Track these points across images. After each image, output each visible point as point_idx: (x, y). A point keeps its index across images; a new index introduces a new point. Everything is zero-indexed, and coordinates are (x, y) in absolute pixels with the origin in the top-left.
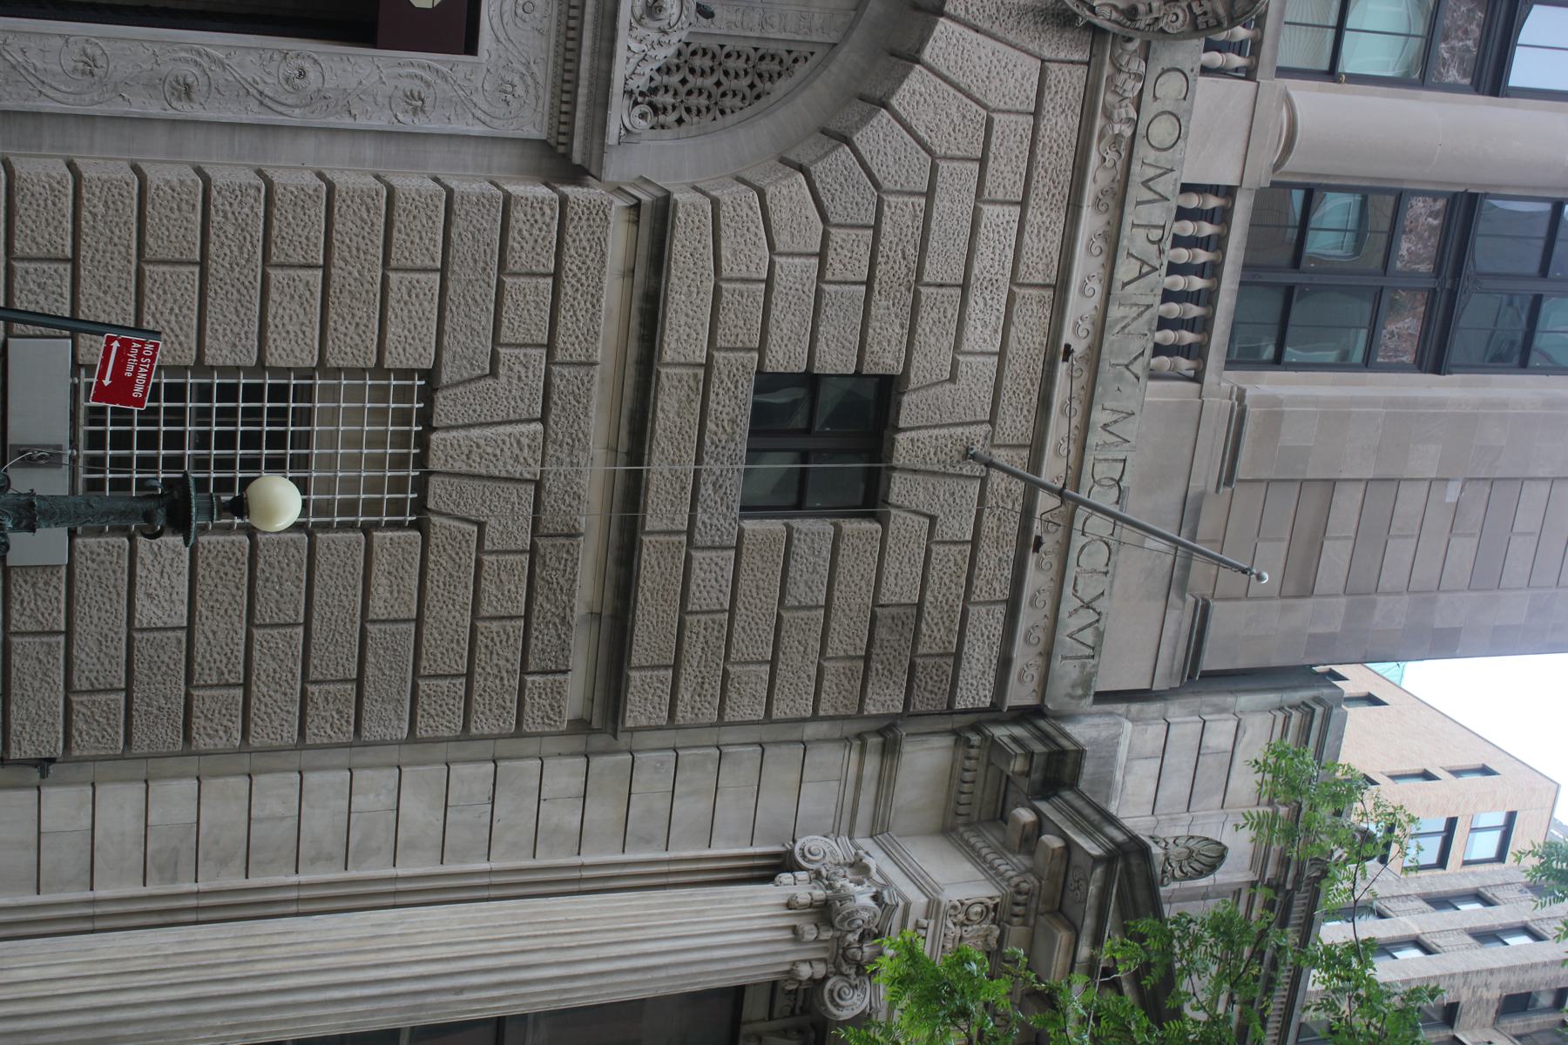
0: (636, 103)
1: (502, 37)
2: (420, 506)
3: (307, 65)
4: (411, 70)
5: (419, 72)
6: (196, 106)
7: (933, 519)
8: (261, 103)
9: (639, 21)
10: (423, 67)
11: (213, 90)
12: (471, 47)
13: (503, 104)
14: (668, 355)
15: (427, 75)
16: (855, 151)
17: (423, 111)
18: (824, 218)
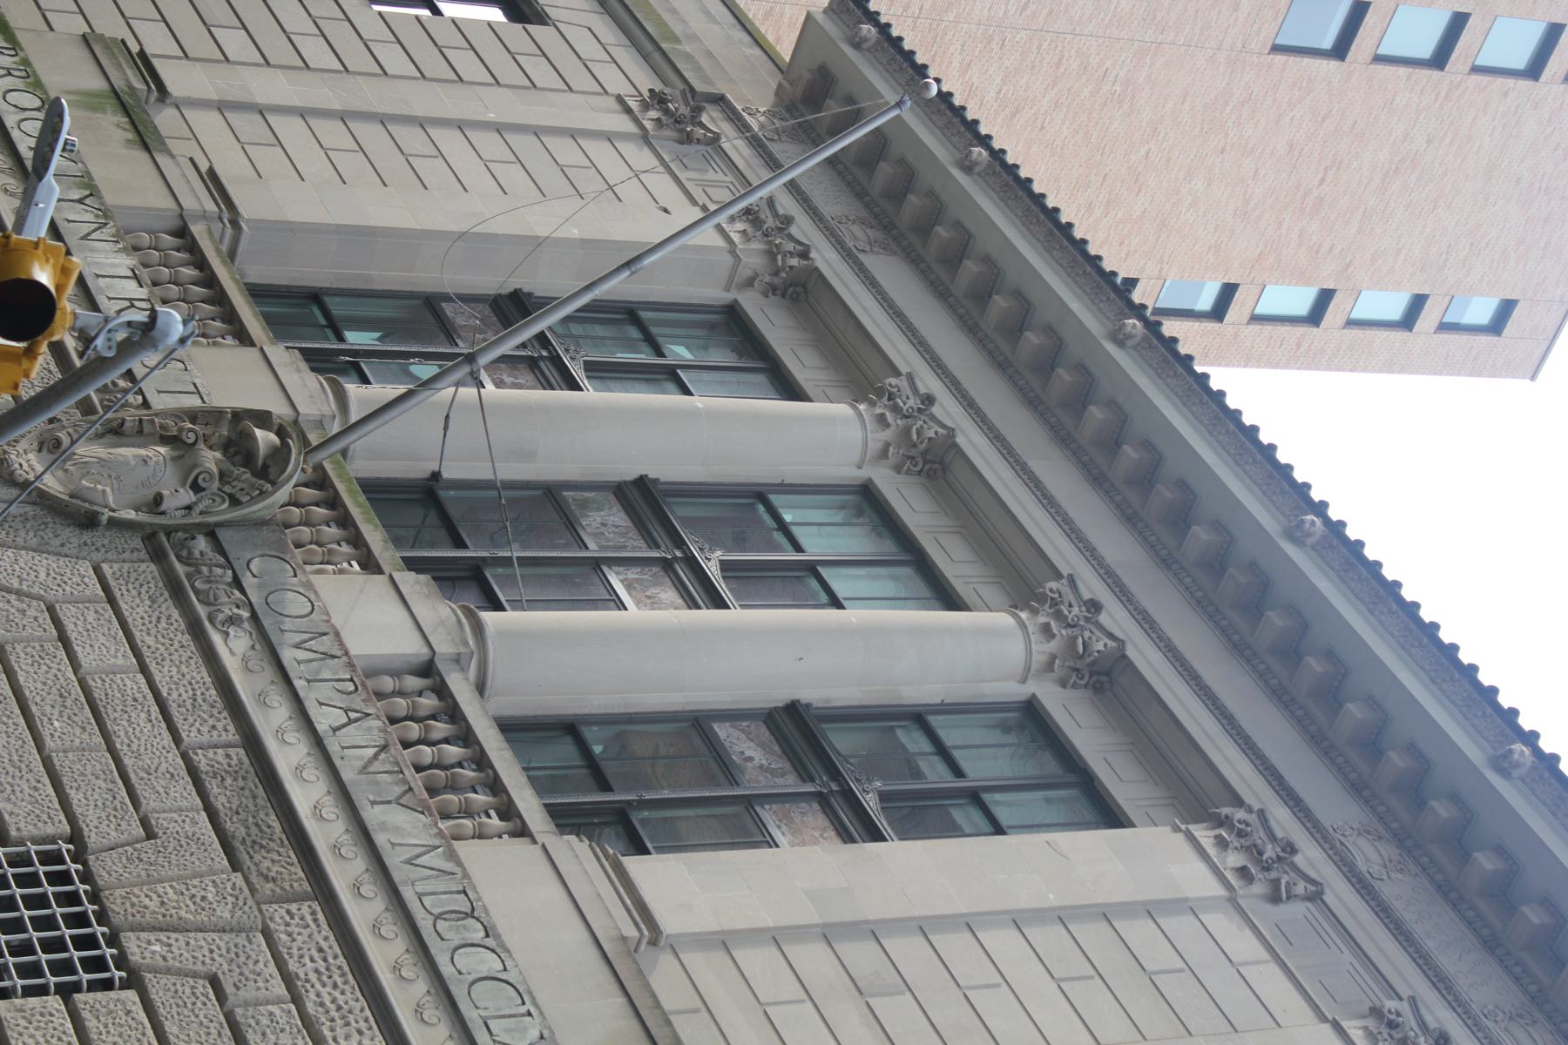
7: (215, 982)
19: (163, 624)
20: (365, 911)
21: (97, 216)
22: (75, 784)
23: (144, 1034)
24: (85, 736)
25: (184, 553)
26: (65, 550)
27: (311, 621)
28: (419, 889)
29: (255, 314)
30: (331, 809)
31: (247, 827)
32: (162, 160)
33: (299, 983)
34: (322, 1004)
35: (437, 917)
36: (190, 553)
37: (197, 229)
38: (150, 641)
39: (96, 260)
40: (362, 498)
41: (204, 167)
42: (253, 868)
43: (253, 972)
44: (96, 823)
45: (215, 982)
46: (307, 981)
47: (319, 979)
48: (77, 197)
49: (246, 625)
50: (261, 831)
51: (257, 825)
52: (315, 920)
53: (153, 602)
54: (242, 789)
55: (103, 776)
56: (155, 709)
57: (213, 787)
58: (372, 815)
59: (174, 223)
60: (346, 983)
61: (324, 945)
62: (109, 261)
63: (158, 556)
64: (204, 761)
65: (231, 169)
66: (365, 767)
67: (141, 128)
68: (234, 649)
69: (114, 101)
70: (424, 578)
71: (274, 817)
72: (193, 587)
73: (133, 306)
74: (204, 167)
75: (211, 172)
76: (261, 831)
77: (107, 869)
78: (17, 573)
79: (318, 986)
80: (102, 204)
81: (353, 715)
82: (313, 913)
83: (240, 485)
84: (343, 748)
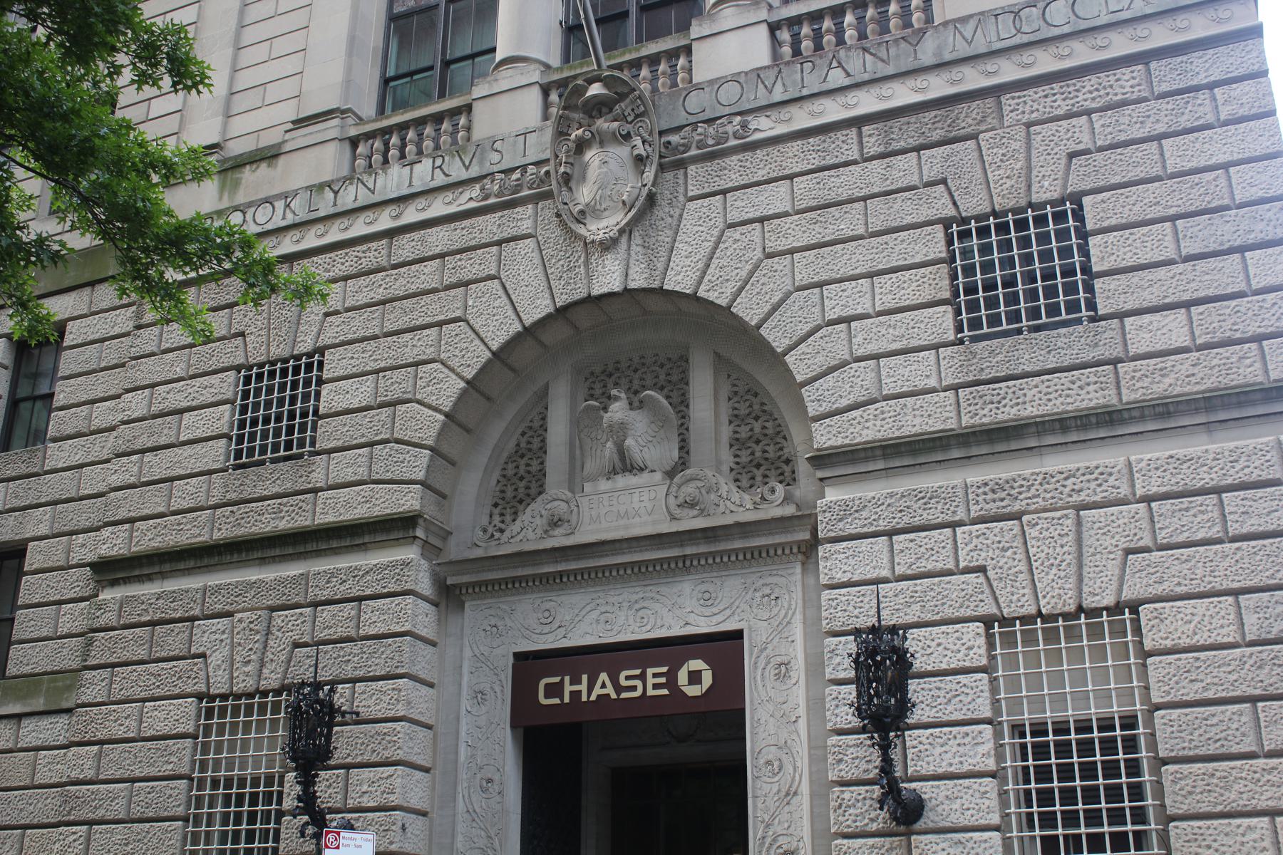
0: (763, 498)
1: (728, 612)
2: (1116, 609)
3: (762, 761)
4: (759, 678)
5: (759, 671)
6: (801, 844)
8: (795, 793)
9: (702, 510)
10: (756, 668)
11: (790, 831)
12: (738, 635)
13: (779, 601)
14: (952, 424)
15: (761, 664)
16: (764, 321)
17: (789, 662)
18: (818, 328)
19: (748, 164)
20: (1008, 71)
21: (351, 184)
22: (899, 220)
23: (1122, 194)
24: (854, 212)
25: (682, 149)
26: (676, 216)
27: (746, 82)
28: (994, 39)
29: (438, 102)
30: (920, 82)
31: (936, 129)
32: (287, 147)
33: (1075, 109)
34: (1093, 99)
35: (1019, 31)
36: (683, 145)
37: (353, 132)
38: (761, 173)
39: (394, 185)
40: (616, 52)
41: (291, 126)
42: (973, 127)
43: (1066, 133)
44: (934, 210)
45: (1072, 155)
46: (1073, 105)
47: (1072, 99)
48: (332, 195)
49: (749, 118)
50: (939, 121)
51: (934, 123)
52: (1019, 97)
53: (725, 169)
54: (900, 129)
55: (891, 204)
56: (826, 173)
57: (896, 146)
58: (927, 58)
59: (347, 147)
60: (1075, 85)
61: (1041, 94)
62: (395, 179)
63: (681, 164)
64: (875, 148)
65: (289, 112)
66: (883, 61)
67: (257, 158)
68: (765, 126)
69: (230, 173)
70: (694, 22)
71: (927, 114)
72: (712, 146)
73: (440, 167)
74: (291, 126)
75: (293, 122)
76: (939, 121)
77: (973, 204)
78: (700, 242)
79: (1078, 100)
80: (338, 180)
81: (835, 64)
82: (1013, 98)
83: (629, 110)
84: (865, 72)
